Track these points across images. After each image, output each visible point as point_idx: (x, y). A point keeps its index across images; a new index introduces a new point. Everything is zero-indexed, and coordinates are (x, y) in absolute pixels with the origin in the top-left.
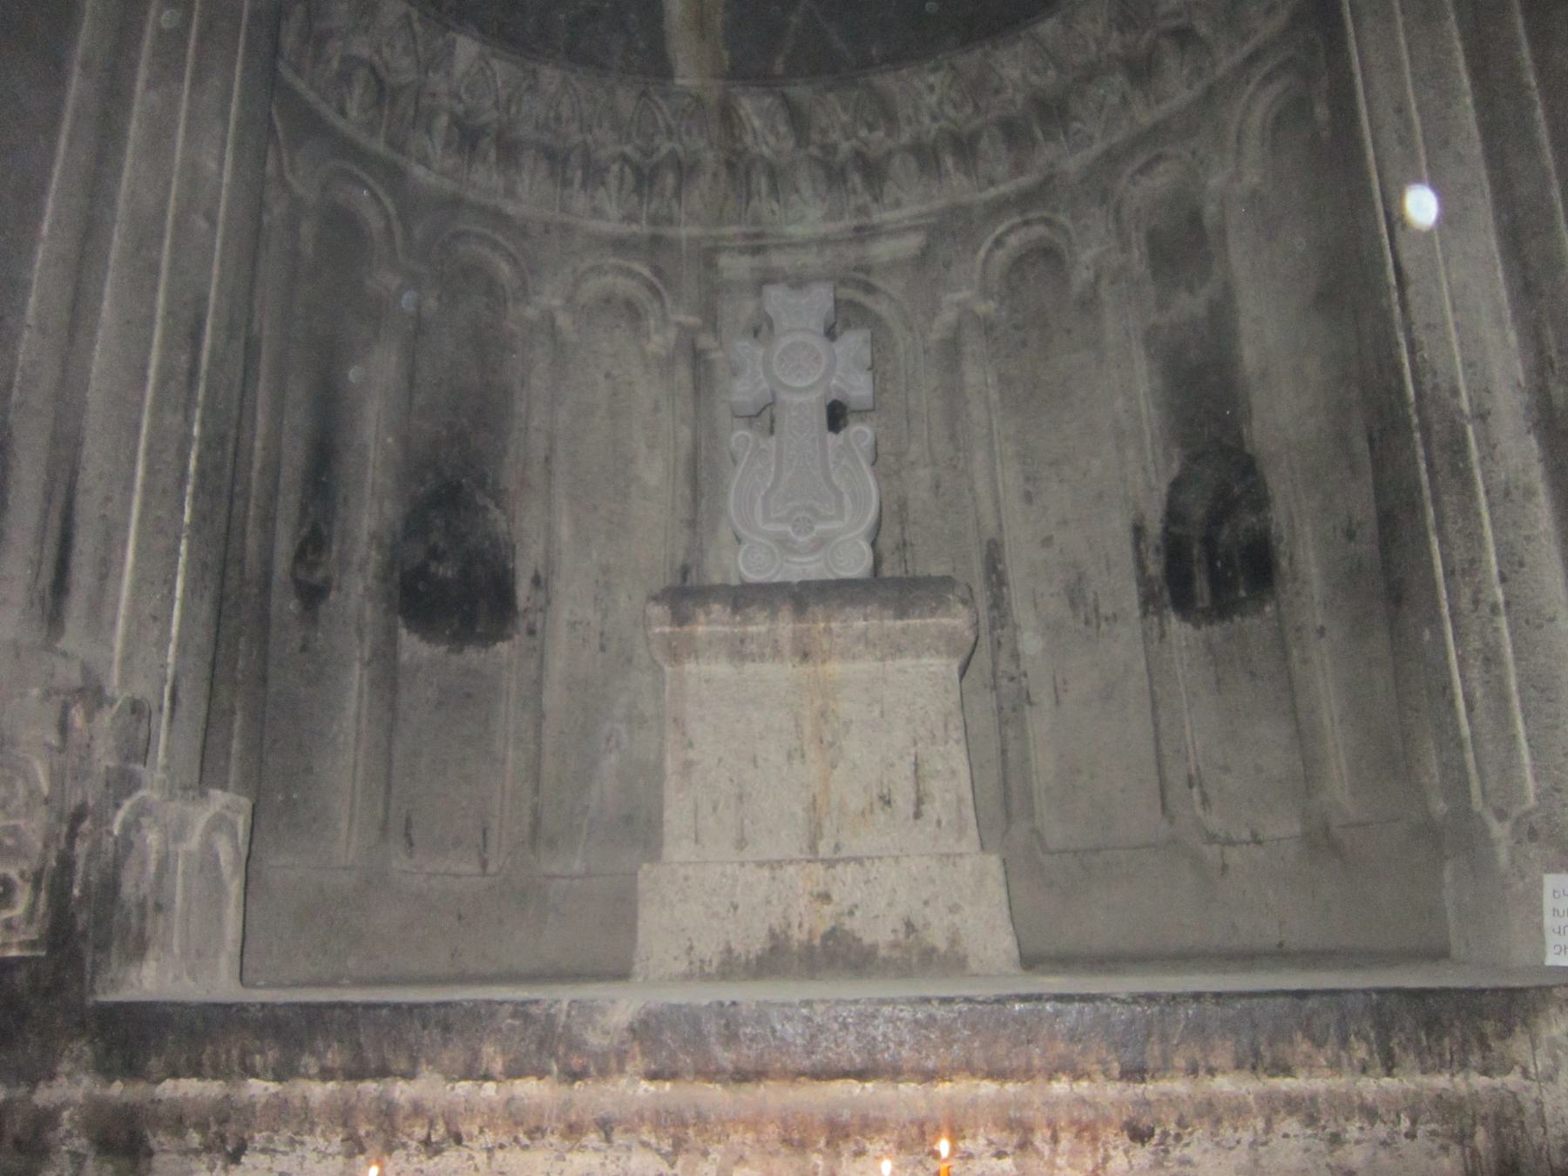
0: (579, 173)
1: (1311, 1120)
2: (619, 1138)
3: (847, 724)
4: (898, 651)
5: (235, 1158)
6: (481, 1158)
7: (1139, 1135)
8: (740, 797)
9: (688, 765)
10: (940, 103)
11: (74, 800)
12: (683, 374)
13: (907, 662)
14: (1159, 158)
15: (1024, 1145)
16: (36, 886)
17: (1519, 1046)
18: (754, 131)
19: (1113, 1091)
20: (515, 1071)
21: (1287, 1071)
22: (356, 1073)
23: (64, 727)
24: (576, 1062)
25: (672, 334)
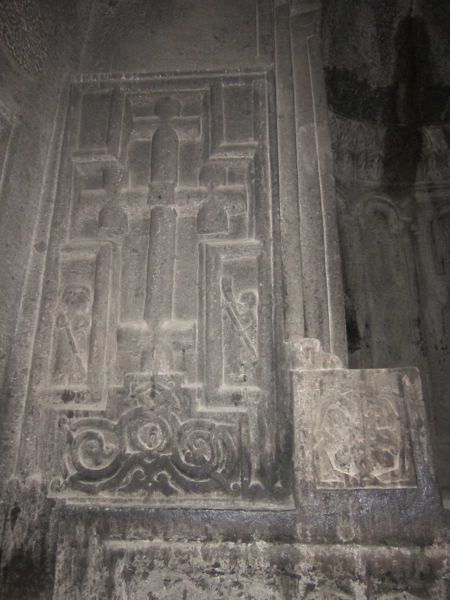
0: (364, 163)
12: (406, 240)
16: (402, 456)
18: (431, 143)
23: (401, 386)
25: (401, 226)
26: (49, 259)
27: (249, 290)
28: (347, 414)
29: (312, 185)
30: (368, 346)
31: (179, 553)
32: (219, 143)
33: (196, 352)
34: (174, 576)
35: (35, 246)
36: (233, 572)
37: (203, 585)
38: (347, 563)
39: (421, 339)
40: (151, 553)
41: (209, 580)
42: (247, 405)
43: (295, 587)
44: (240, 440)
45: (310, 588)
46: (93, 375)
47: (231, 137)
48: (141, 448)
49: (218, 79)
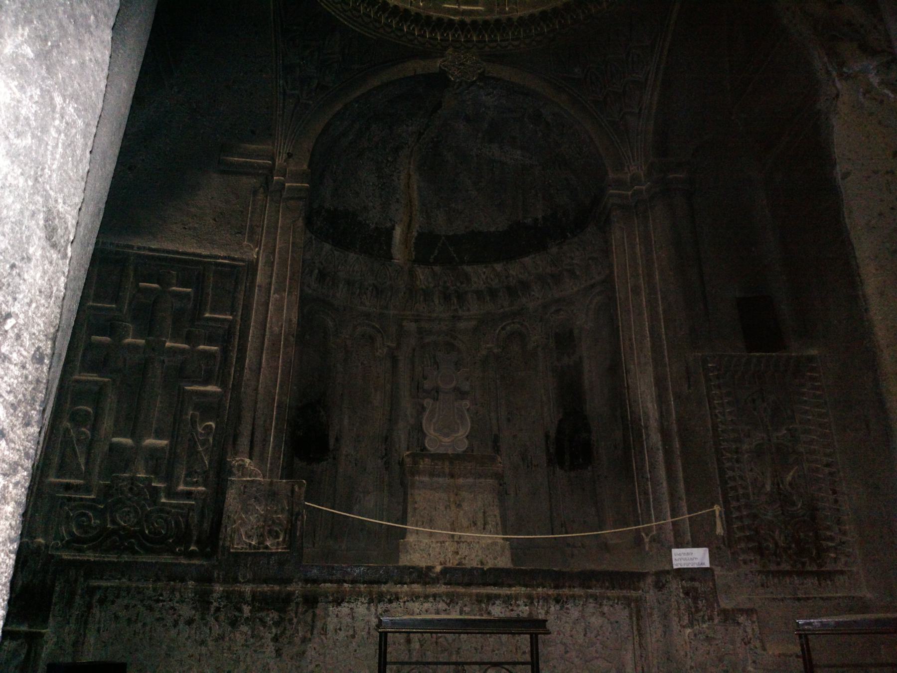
1: (596, 599)
2: (437, 599)
4: (480, 476)
5: (339, 604)
6: (402, 604)
7: (557, 601)
8: (431, 520)
9: (415, 509)
10: (487, 278)
11: (296, 509)
13: (482, 480)
15: (532, 603)
16: (285, 534)
17: (642, 584)
19: (551, 592)
20: (413, 583)
21: (590, 588)
22: (371, 582)
24: (427, 580)
25: (385, 350)
29: (275, 344)
30: (334, 458)
31: (137, 587)
33: (166, 462)
36: (171, 600)
38: (241, 594)
39: (386, 454)
40: (119, 588)
41: (155, 605)
42: (195, 499)
43: (208, 609)
44: (187, 521)
45: (218, 609)
47: (213, 311)
48: (119, 524)
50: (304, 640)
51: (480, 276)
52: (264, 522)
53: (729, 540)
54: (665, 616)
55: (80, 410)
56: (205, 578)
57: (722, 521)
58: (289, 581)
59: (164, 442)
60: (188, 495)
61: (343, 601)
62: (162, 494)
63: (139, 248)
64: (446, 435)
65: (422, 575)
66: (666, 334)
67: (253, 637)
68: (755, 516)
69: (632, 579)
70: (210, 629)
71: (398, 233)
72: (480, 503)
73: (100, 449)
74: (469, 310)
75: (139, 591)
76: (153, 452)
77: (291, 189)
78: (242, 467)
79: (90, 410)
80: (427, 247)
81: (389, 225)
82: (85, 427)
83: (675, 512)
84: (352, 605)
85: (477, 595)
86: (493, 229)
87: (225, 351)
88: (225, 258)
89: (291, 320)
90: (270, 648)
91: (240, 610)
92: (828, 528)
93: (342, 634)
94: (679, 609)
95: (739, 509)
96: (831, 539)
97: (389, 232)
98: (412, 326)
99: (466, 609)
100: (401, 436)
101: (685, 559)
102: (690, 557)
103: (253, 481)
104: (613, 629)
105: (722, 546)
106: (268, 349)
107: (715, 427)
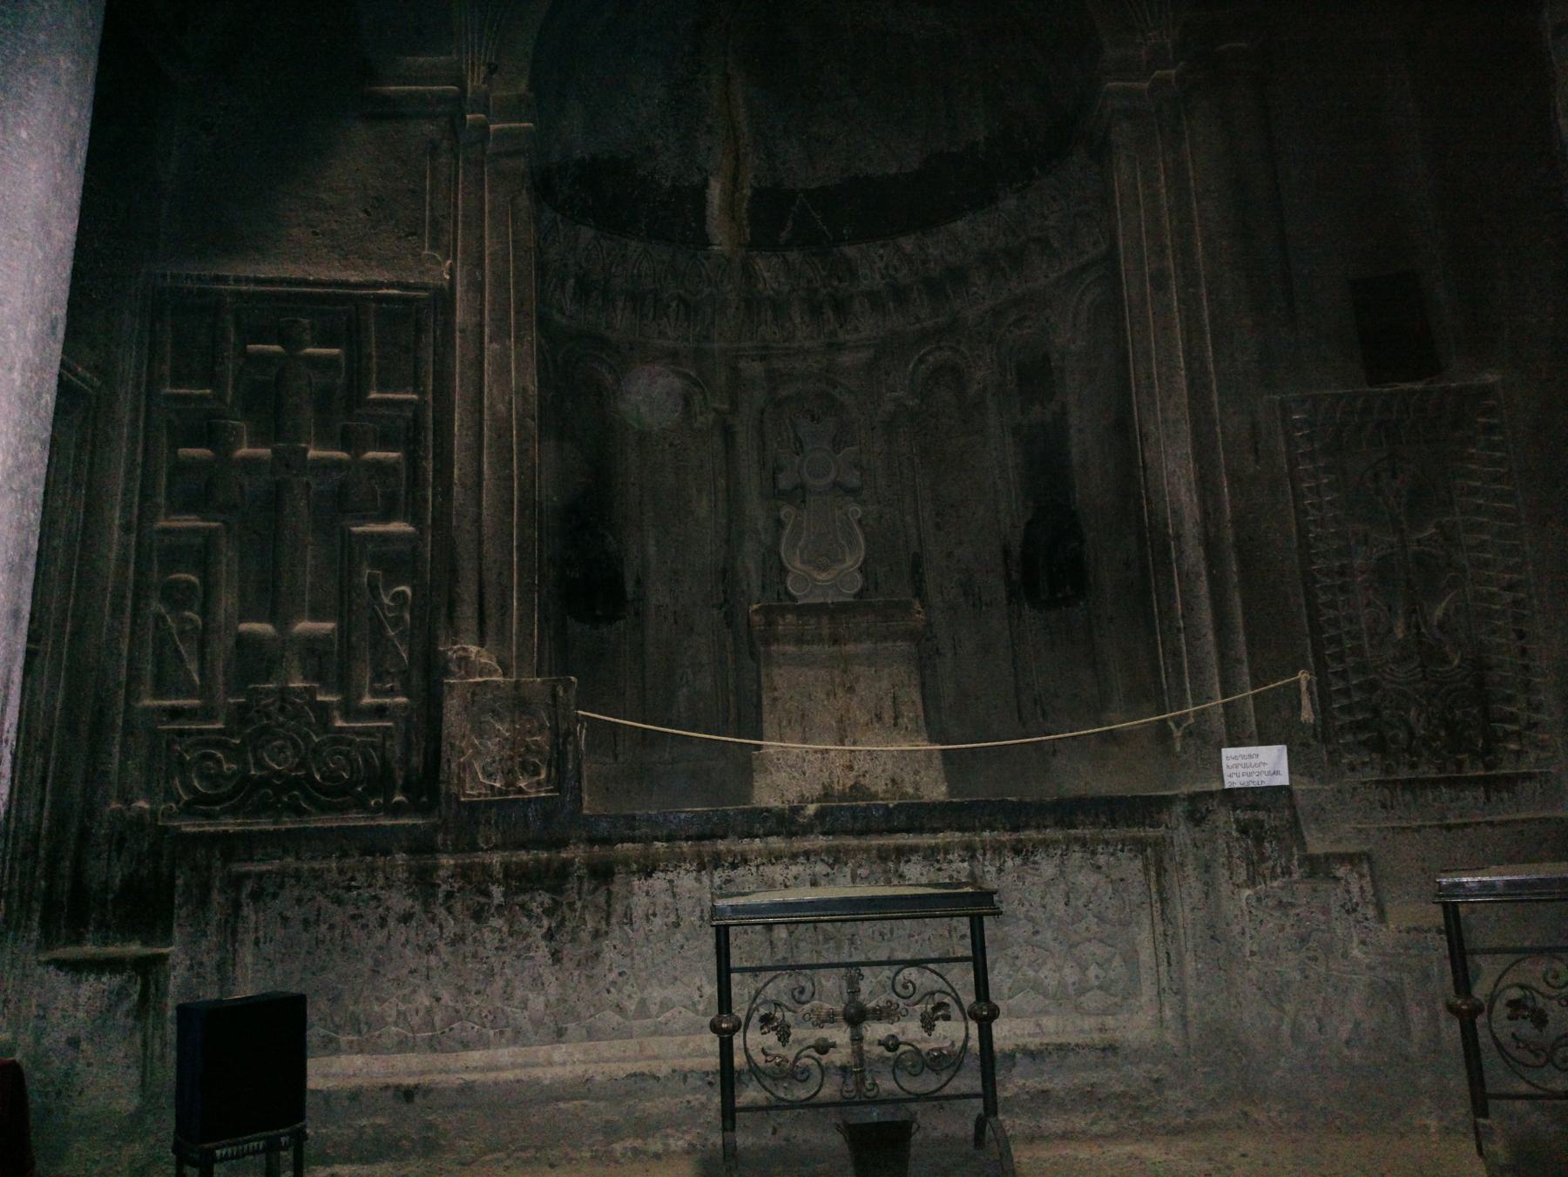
1: (1084, 845)
2: (812, 859)
3: (857, 679)
4: (885, 638)
5: (649, 875)
6: (754, 870)
7: (1017, 851)
10: (886, 268)
11: (563, 726)
13: (889, 644)
14: (1024, 318)
15: (973, 857)
16: (549, 766)
19: (1006, 837)
20: (767, 835)
22: (700, 837)
24: (794, 829)
25: (712, 416)
26: (139, 544)
27: (402, 588)
28: (498, 726)
29: (502, 433)
30: (637, 614)
32: (367, 394)
34: (308, 894)
35: (121, 526)
36: (370, 886)
37: (339, 901)
38: (486, 868)
39: (726, 600)
40: (282, 873)
43: (435, 895)
46: (206, 690)
47: (383, 387)
49: (364, 298)
50: (596, 934)
51: (873, 263)
52: (512, 749)
53: (1325, 732)
54: (1207, 868)
55: (177, 581)
56: (422, 846)
57: (1312, 700)
58: (562, 844)
59: (329, 626)
60: (380, 712)
61: (654, 870)
62: (336, 713)
63: (238, 280)
64: (823, 568)
65: (786, 822)
66: (1216, 362)
67: (511, 935)
68: (1373, 686)
69: (1146, 809)
70: (441, 927)
71: (715, 192)
72: (885, 684)
73: (221, 648)
74: (856, 329)
75: (317, 875)
76: (311, 646)
77: (502, 135)
78: (464, 660)
79: (193, 578)
80: (772, 216)
81: (696, 179)
82: (190, 609)
83: (1227, 687)
84: (670, 876)
85: (880, 849)
86: (893, 170)
87: (413, 460)
88: (391, 285)
89: (525, 390)
90: (542, 952)
91: (488, 895)
92: (1509, 700)
93: (658, 922)
94: (1230, 856)
95: (1343, 675)
96: (1512, 719)
97: (700, 193)
98: (757, 368)
99: (862, 872)
100: (750, 563)
101: (1245, 766)
102: (1254, 761)
103: (485, 682)
104: (1115, 891)
105: (1312, 741)
106: (490, 446)
107: (1302, 533)
